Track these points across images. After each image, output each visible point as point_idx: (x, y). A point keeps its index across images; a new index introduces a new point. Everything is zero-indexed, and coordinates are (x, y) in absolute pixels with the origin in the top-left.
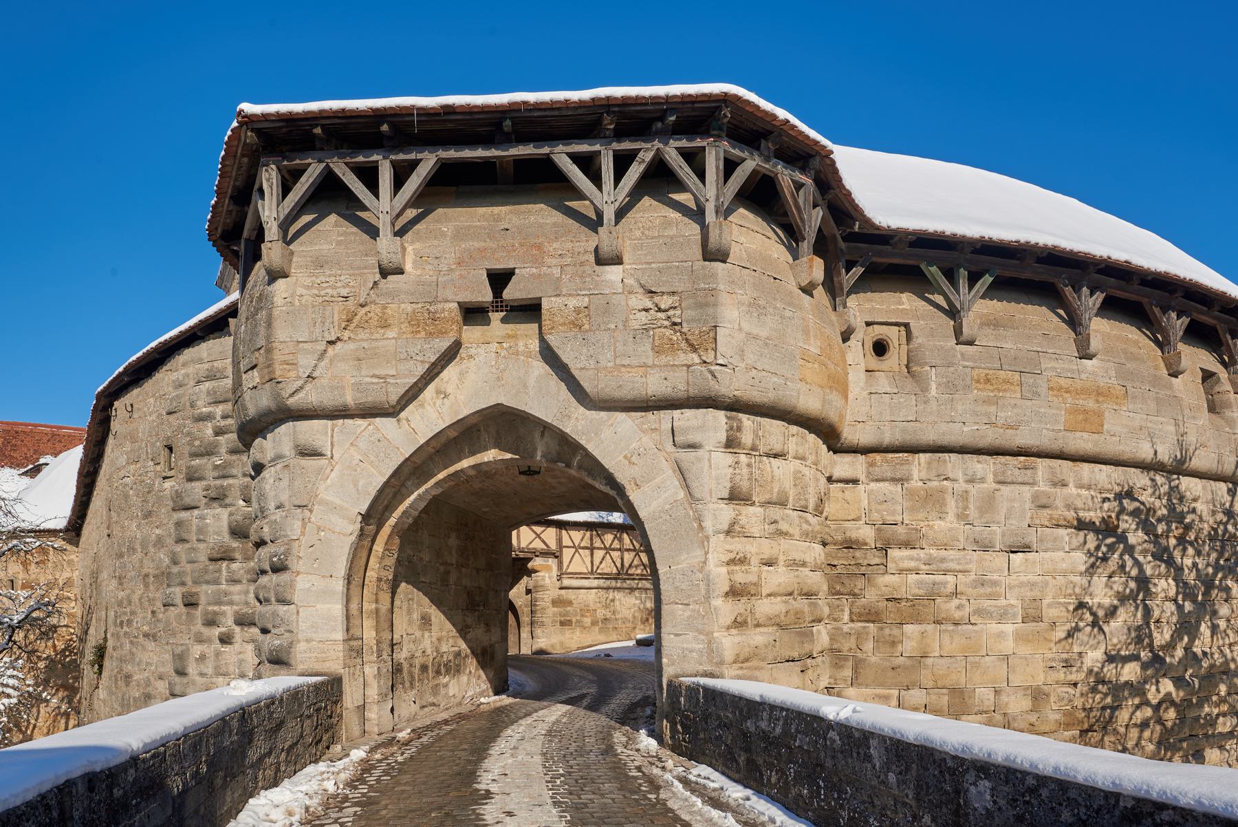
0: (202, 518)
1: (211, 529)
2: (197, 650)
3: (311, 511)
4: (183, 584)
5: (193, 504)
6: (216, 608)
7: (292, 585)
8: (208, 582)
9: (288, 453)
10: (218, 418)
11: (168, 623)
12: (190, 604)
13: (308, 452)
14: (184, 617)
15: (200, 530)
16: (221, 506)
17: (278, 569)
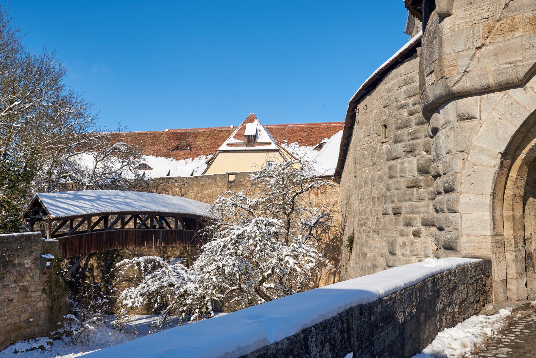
0: (402, 163)
1: (407, 170)
2: (401, 240)
3: (468, 154)
4: (393, 202)
5: (398, 156)
6: (411, 216)
7: (457, 200)
8: (406, 201)
9: (453, 120)
10: (410, 105)
11: (385, 225)
12: (397, 213)
13: (465, 118)
14: (393, 221)
15: (402, 171)
16: (413, 156)
17: (448, 191)
